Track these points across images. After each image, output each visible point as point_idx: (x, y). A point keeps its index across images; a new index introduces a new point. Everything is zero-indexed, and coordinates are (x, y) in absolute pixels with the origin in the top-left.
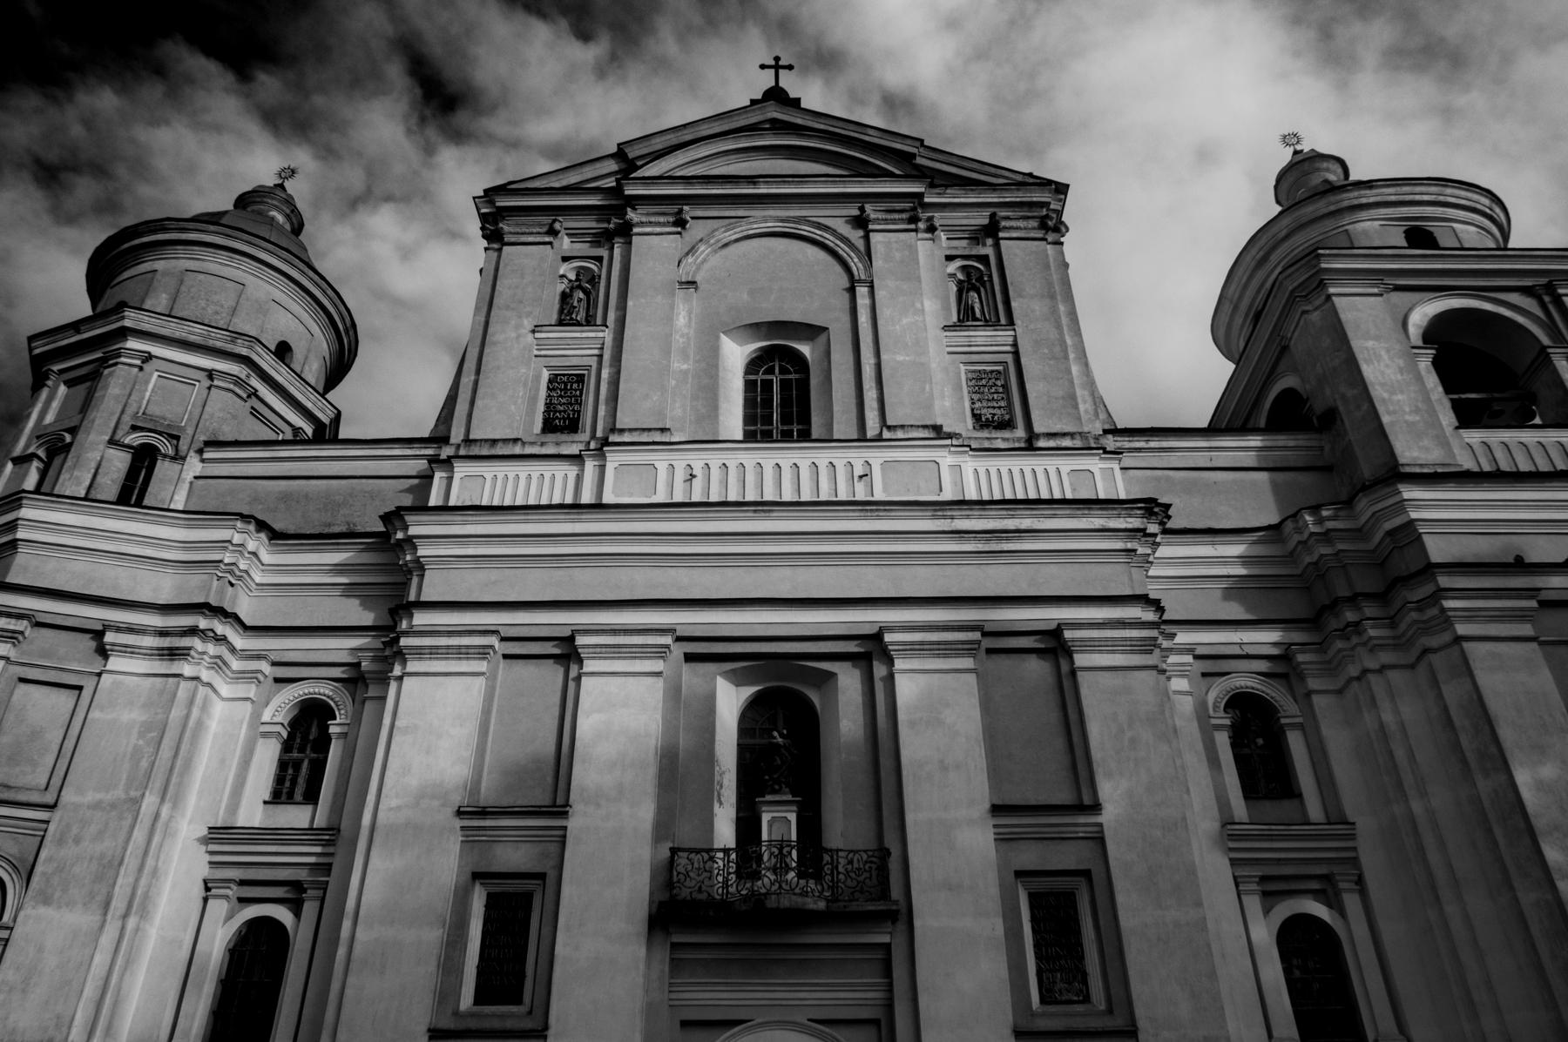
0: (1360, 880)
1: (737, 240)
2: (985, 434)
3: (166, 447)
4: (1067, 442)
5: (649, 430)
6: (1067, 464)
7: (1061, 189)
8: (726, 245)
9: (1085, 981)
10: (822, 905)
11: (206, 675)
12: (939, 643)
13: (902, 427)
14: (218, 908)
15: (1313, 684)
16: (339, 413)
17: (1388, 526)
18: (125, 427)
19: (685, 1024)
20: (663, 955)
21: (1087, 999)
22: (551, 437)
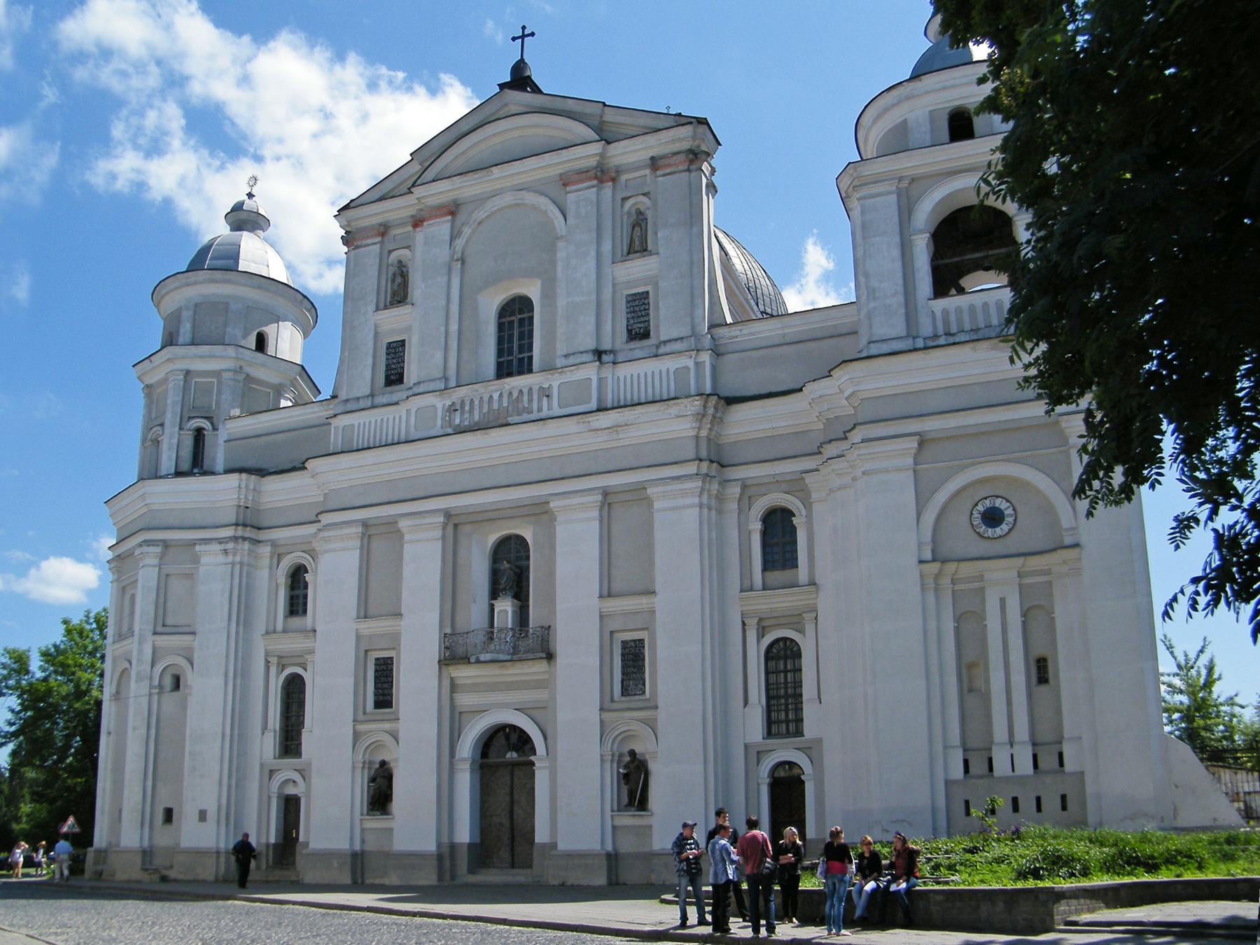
2: (633, 345)
3: (205, 424)
6: (670, 364)
10: (509, 657)
11: (246, 559)
15: (814, 496)
20: (446, 683)
21: (644, 692)
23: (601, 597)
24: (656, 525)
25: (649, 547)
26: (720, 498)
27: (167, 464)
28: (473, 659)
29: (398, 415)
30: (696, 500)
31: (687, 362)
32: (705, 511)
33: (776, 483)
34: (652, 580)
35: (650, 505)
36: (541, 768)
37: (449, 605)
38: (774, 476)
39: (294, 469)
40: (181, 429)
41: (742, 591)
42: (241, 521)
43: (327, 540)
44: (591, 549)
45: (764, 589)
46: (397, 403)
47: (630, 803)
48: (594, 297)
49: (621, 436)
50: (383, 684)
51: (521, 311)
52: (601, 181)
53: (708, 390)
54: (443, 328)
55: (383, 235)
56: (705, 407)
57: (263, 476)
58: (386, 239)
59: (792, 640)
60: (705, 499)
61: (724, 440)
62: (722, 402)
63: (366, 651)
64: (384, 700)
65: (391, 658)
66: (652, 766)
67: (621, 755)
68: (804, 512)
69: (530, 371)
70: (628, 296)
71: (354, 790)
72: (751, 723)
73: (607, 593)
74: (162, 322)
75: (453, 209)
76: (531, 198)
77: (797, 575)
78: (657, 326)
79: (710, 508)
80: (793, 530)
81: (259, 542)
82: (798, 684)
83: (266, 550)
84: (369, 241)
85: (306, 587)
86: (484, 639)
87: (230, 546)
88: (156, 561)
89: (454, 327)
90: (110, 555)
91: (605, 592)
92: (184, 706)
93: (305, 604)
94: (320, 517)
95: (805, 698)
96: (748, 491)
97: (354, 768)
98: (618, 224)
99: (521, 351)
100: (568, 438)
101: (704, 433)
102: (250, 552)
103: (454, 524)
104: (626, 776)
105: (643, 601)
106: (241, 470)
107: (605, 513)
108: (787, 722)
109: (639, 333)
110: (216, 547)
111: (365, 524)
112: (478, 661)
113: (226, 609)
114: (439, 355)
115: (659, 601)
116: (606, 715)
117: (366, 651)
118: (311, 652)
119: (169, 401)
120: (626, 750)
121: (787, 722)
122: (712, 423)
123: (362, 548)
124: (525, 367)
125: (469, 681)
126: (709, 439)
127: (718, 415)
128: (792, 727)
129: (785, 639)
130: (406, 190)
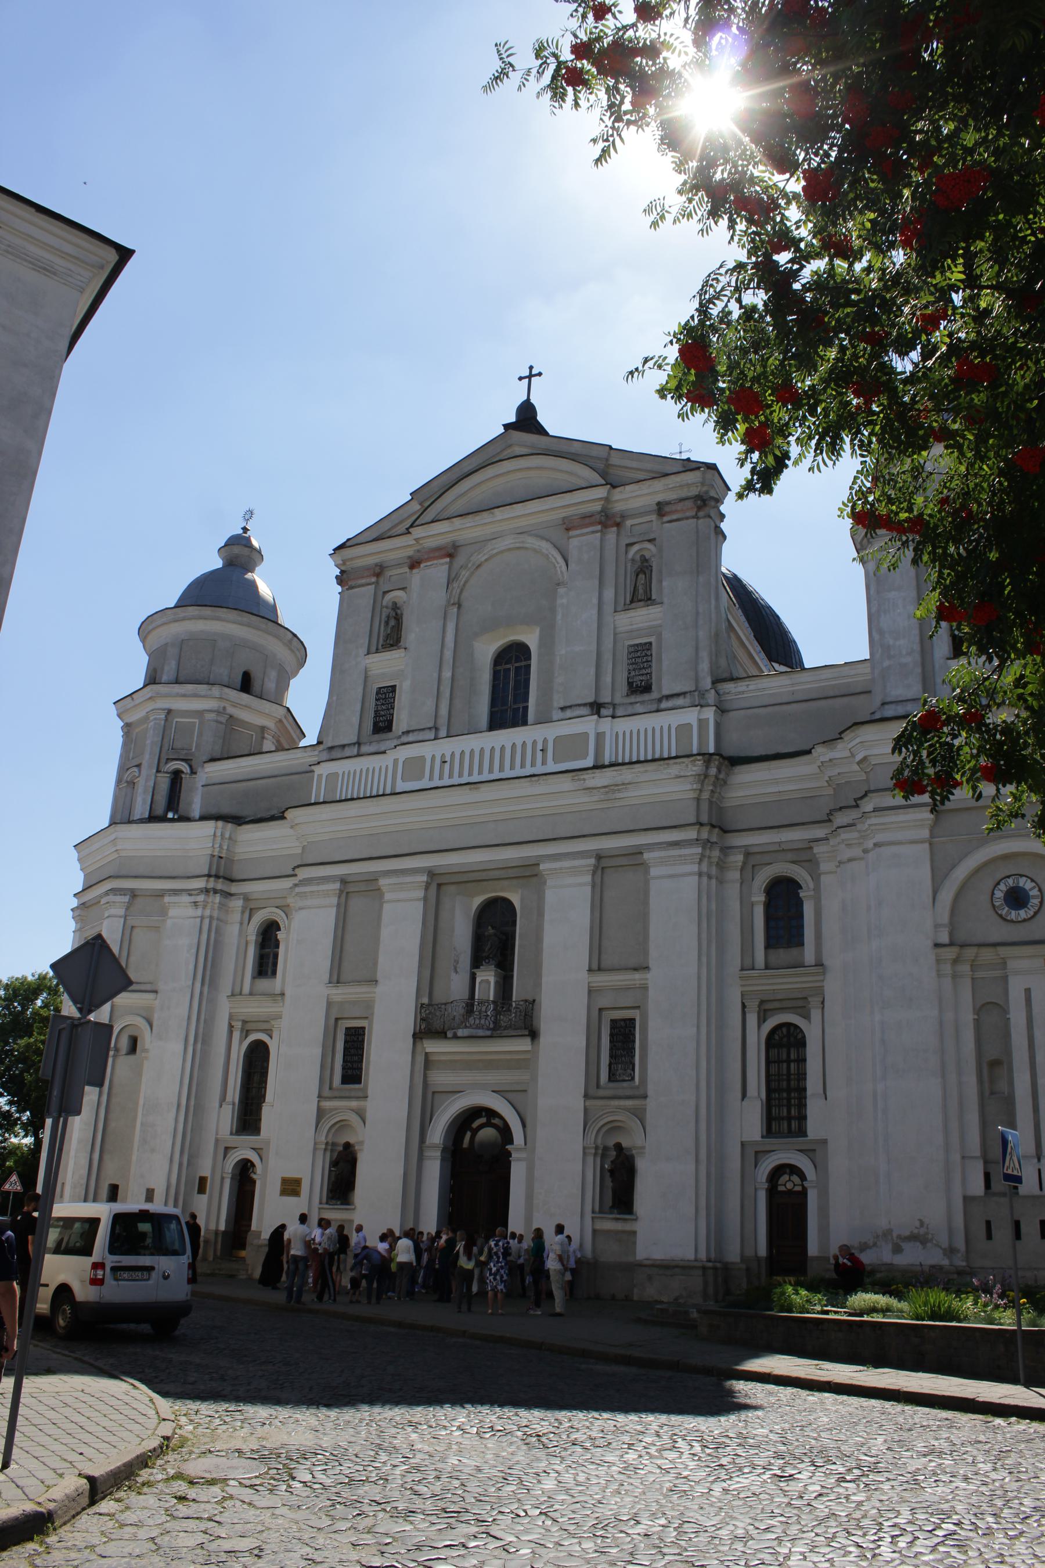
0: (823, 1002)
1: (486, 560)
2: (632, 699)
4: (680, 701)
5: (423, 729)
7: (713, 467)
8: (479, 566)
9: (633, 1070)
10: (489, 1033)
11: (215, 914)
12: (570, 868)
13: (570, 707)
14: (236, 1035)
15: (824, 867)
16: (288, 709)
17: (859, 757)
18: (163, 761)
19: (434, 1093)
20: (420, 1059)
21: (633, 1079)
22: (377, 736)
23: (590, 970)
24: (652, 893)
25: (644, 917)
26: (721, 866)
27: (141, 809)
28: (450, 1034)
29: (381, 765)
30: (695, 868)
31: (690, 716)
32: (705, 879)
33: (781, 851)
34: (646, 953)
35: (647, 871)
36: (519, 1160)
37: (427, 973)
38: (780, 843)
39: (272, 818)
40: (158, 771)
41: (742, 969)
42: (213, 873)
43: (302, 895)
44: (581, 917)
45: (767, 968)
46: (384, 752)
47: (613, 1207)
48: (594, 647)
49: (621, 795)
50: (351, 1054)
51: (518, 660)
52: (605, 525)
53: (712, 750)
54: (436, 675)
55: (378, 575)
56: (707, 768)
57: (240, 825)
58: (381, 580)
59: (796, 1027)
60: (704, 868)
61: (727, 804)
62: (726, 762)
63: (337, 1019)
64: (353, 1072)
65: (363, 1028)
66: (641, 1164)
67: (606, 1149)
68: (811, 885)
69: (525, 723)
70: (631, 646)
71: (311, 1171)
72: (748, 1120)
73: (597, 967)
74: (145, 659)
75: (451, 551)
76: (531, 542)
77: (802, 954)
78: (660, 679)
79: (710, 877)
80: (799, 903)
81: (231, 895)
82: (802, 1076)
83: (237, 904)
84: (363, 581)
85: (277, 946)
86: (462, 1011)
87: (201, 898)
88: (122, 912)
89: (447, 674)
90: (75, 903)
91: (595, 966)
92: (138, 1072)
93: (275, 964)
94: (297, 871)
95: (809, 1092)
96: (752, 859)
97: (315, 1149)
98: (622, 572)
99: (515, 702)
100: (564, 797)
101: (706, 795)
102: (222, 906)
103: (438, 884)
104: (612, 1172)
105: (637, 976)
106: (217, 818)
107: (598, 880)
108: (789, 1119)
109: (640, 687)
110: (186, 899)
111: (344, 881)
112: (455, 1037)
113: (191, 967)
114: (430, 703)
115: (654, 978)
116: (589, 1103)
117: (337, 1019)
118: (279, 1017)
119: (148, 742)
120: (611, 1143)
121: (789, 1119)
122: (714, 785)
123: (338, 905)
124: (519, 719)
125: (443, 1058)
126: (711, 802)
127: (721, 776)
128: (794, 1124)
129: (788, 1025)
130: (402, 528)
